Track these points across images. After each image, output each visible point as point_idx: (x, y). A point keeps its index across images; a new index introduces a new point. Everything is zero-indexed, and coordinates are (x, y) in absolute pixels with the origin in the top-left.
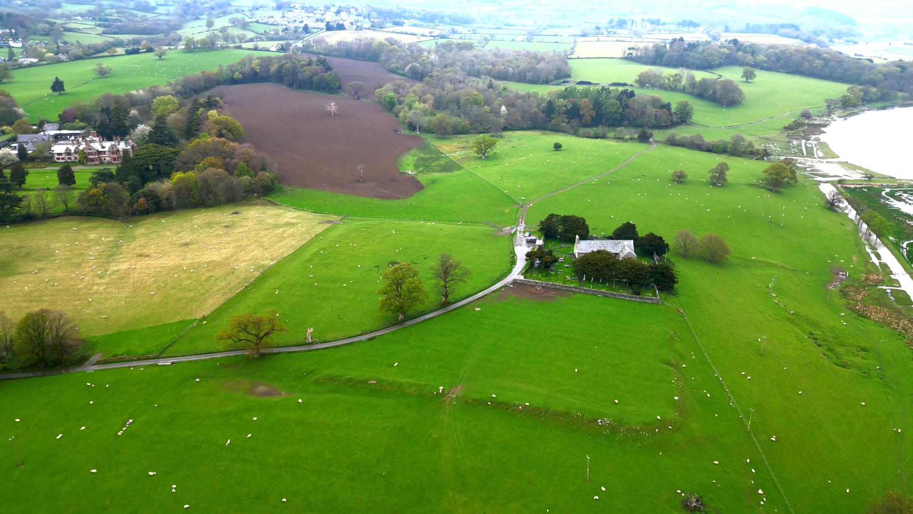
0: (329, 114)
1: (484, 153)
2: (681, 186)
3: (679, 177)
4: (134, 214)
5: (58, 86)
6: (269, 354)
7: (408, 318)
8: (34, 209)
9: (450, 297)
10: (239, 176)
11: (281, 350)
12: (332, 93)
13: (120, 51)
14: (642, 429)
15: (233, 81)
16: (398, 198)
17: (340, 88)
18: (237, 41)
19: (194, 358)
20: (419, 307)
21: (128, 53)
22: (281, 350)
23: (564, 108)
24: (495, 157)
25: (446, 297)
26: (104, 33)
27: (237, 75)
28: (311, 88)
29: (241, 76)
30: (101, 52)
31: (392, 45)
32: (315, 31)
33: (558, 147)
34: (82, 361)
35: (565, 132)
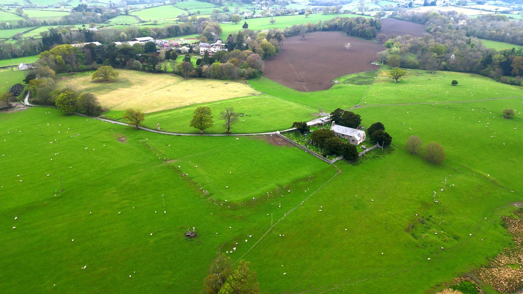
0: (345, 49)
1: (396, 79)
2: (508, 121)
3: (508, 114)
4: (190, 77)
5: (245, 26)
6: (141, 129)
7: (204, 133)
8: (163, 69)
9: (231, 130)
10: (242, 68)
11: (150, 130)
12: (368, 40)
13: (297, 13)
14: (216, 201)
15: (324, 30)
16: (305, 91)
17: (374, 36)
18: (364, 10)
19: (124, 124)
20: (207, 130)
21: (300, 14)
22: (150, 130)
23: (498, 61)
24: (402, 82)
25: (229, 130)
26: (309, 5)
27: (326, 26)
28: (357, 36)
29: (328, 27)
30: (290, 13)
31: (442, 15)
32: (415, 6)
33: (454, 83)
34: (97, 115)
35: (492, 77)
